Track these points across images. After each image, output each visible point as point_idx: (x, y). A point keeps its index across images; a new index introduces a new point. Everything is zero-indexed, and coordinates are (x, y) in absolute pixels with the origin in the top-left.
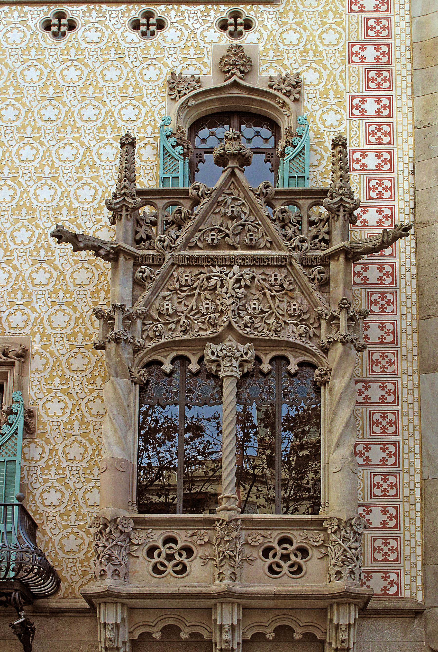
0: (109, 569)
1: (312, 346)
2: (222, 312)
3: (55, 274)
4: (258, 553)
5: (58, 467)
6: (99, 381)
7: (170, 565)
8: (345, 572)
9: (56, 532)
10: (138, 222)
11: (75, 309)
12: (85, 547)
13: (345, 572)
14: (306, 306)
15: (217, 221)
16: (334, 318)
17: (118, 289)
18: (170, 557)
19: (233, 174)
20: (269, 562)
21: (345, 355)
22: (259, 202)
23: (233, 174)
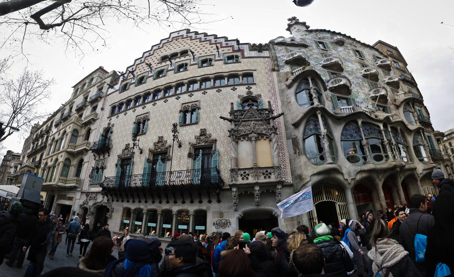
0: (233, 179)
1: (268, 134)
2: (251, 129)
3: (221, 126)
4: (261, 174)
5: (223, 161)
6: (229, 144)
7: (245, 178)
8: (279, 177)
9: (223, 173)
10: (235, 115)
11: (224, 132)
12: (228, 176)
13: (279, 177)
14: (266, 127)
15: (249, 114)
16: (271, 129)
17: (232, 126)
18: (245, 176)
19: (251, 107)
20: (264, 176)
21: (274, 135)
22: (256, 111)
23: (251, 107)
